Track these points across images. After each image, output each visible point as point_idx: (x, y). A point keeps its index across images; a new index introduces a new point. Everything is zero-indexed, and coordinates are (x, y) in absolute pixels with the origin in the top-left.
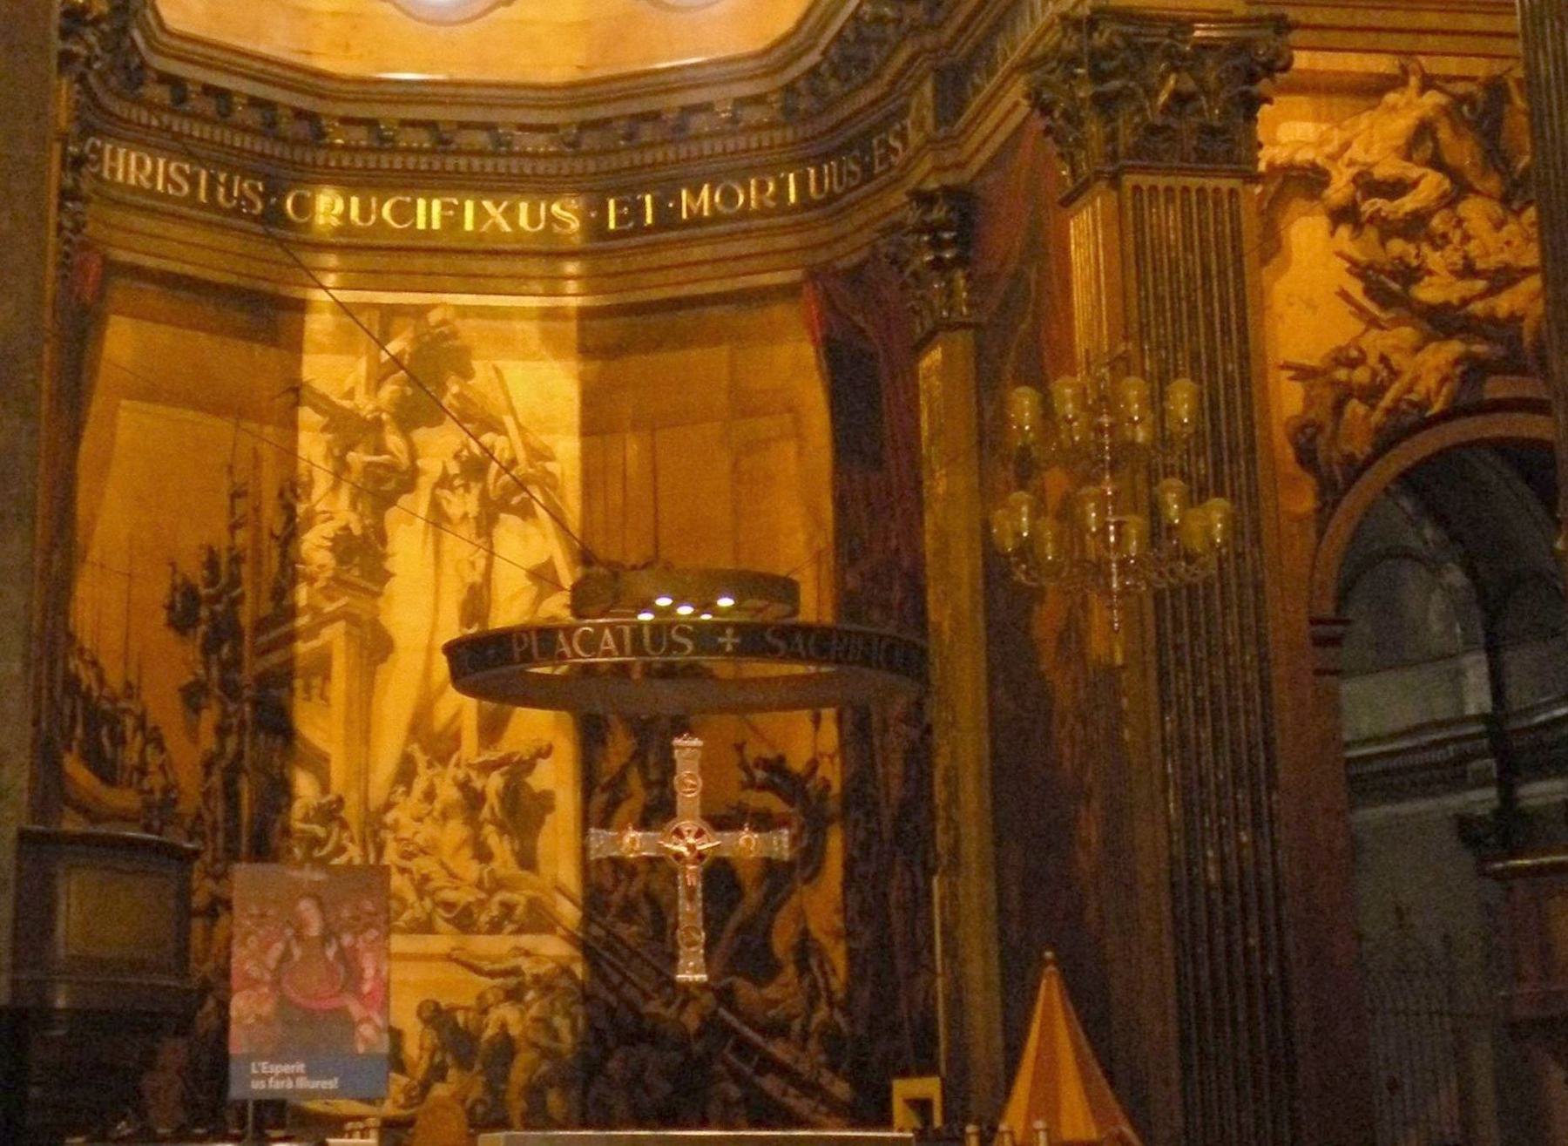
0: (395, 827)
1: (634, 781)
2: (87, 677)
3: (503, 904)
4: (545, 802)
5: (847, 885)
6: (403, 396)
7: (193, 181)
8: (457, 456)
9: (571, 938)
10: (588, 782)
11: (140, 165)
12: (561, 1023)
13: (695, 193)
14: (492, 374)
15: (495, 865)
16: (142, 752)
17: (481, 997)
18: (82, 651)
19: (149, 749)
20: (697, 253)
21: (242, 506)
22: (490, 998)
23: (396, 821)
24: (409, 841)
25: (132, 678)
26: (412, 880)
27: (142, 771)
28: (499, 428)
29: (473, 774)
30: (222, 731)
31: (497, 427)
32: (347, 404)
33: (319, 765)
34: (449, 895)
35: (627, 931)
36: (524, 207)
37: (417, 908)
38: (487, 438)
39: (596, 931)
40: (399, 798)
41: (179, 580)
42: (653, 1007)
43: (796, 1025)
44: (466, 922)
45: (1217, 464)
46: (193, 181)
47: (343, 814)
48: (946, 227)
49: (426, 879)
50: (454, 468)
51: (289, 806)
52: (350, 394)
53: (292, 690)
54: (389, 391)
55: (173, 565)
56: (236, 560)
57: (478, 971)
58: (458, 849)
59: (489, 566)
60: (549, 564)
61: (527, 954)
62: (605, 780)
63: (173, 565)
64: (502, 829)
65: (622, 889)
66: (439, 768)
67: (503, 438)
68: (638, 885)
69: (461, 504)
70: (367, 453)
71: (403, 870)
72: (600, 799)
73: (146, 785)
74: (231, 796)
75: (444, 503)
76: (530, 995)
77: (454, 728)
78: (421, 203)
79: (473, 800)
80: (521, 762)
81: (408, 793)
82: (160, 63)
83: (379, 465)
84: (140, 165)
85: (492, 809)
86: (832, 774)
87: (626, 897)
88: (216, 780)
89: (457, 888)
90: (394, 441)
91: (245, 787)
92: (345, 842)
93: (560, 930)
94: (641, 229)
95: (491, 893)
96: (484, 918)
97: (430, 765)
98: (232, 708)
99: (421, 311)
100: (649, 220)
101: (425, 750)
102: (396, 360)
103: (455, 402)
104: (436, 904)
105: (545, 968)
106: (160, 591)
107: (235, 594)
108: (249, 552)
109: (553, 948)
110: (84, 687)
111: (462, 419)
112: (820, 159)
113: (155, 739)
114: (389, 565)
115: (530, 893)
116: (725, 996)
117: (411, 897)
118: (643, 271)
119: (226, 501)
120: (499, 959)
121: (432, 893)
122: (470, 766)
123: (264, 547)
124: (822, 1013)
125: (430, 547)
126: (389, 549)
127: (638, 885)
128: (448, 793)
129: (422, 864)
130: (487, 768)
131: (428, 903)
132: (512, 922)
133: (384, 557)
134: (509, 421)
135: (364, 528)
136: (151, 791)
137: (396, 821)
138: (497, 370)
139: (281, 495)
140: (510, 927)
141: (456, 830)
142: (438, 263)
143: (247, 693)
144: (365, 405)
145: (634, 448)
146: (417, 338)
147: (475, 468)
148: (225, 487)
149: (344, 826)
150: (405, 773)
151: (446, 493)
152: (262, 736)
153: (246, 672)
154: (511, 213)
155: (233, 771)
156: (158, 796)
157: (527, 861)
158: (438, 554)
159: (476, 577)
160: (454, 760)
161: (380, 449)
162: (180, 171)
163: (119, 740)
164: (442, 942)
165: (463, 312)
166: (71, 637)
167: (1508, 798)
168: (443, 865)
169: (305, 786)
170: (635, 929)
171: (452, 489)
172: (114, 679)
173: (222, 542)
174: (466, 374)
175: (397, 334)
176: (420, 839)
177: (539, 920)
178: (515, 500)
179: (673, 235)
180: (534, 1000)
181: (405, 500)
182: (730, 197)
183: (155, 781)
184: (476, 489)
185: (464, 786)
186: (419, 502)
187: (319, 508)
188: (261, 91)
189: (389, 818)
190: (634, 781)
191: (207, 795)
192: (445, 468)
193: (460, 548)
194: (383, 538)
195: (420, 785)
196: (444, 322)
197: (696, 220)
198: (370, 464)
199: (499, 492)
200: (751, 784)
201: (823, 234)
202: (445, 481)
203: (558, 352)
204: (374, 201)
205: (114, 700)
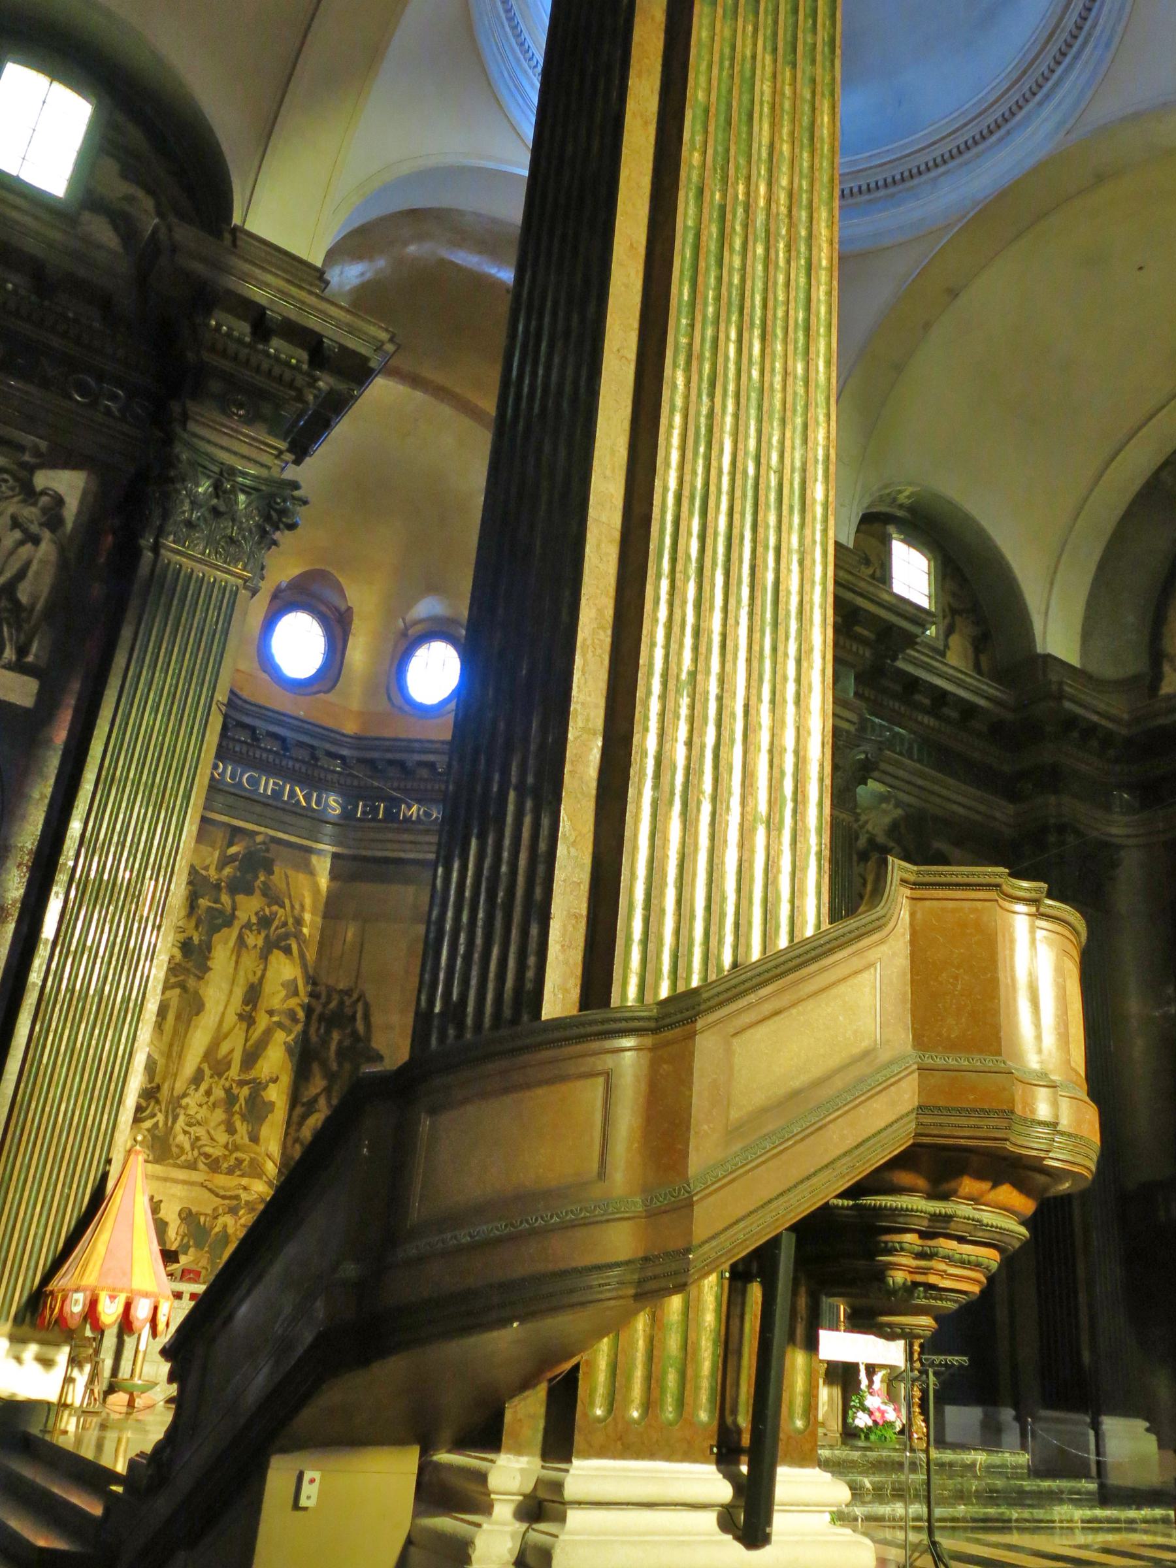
0: (186, 1108)
1: (322, 1102)
3: (236, 1159)
6: (235, 877)
8: (257, 914)
9: (269, 1183)
10: (294, 1100)
14: (283, 876)
15: (237, 1137)
17: (215, 1210)
20: (406, 837)
23: (188, 1104)
26: (190, 1138)
29: (234, 1085)
32: (204, 872)
34: (208, 1150)
37: (190, 1156)
38: (275, 908)
47: (158, 1095)
49: (198, 1139)
50: (254, 920)
52: (206, 868)
54: (228, 871)
57: (217, 1195)
58: (219, 1124)
59: (263, 976)
61: (245, 1188)
62: (305, 1100)
64: (244, 1118)
67: (282, 910)
69: (255, 940)
70: (209, 901)
71: (185, 1132)
72: (299, 1110)
75: (246, 937)
76: (241, 1212)
77: (226, 1060)
79: (231, 1099)
81: (196, 1090)
83: (216, 909)
85: (241, 1105)
90: (225, 898)
92: (156, 1111)
93: (264, 1178)
94: (375, 819)
95: (231, 1152)
96: (225, 1165)
97: (212, 1077)
99: (254, 834)
100: (381, 816)
101: (210, 1068)
102: (233, 858)
103: (261, 886)
104: (200, 1154)
111: (265, 894)
114: (209, 963)
115: (253, 1155)
117: (187, 1147)
118: (373, 840)
120: (229, 1189)
122: (233, 1080)
125: (234, 958)
126: (211, 955)
128: (219, 1093)
129: (199, 1131)
130: (242, 1083)
131: (196, 1153)
132: (240, 1170)
133: (208, 958)
134: (287, 901)
135: (200, 940)
137: (188, 1104)
138: (287, 876)
141: (219, 1115)
144: (212, 874)
146: (247, 848)
147: (265, 922)
149: (158, 1102)
150: (197, 1079)
151: (248, 932)
157: (254, 1139)
158: (237, 962)
159: (256, 980)
160: (225, 1077)
161: (217, 901)
164: (196, 1176)
165: (274, 840)
168: (208, 1132)
171: (251, 931)
174: (270, 872)
175: (237, 844)
176: (199, 1117)
177: (256, 1170)
178: (283, 944)
180: (244, 1215)
181: (225, 930)
184: (263, 934)
185: (228, 1091)
186: (234, 933)
189: (184, 1102)
192: (249, 920)
193: (249, 961)
194: (209, 949)
195: (203, 1087)
196: (264, 843)
197: (407, 820)
199: (275, 938)
202: (248, 926)
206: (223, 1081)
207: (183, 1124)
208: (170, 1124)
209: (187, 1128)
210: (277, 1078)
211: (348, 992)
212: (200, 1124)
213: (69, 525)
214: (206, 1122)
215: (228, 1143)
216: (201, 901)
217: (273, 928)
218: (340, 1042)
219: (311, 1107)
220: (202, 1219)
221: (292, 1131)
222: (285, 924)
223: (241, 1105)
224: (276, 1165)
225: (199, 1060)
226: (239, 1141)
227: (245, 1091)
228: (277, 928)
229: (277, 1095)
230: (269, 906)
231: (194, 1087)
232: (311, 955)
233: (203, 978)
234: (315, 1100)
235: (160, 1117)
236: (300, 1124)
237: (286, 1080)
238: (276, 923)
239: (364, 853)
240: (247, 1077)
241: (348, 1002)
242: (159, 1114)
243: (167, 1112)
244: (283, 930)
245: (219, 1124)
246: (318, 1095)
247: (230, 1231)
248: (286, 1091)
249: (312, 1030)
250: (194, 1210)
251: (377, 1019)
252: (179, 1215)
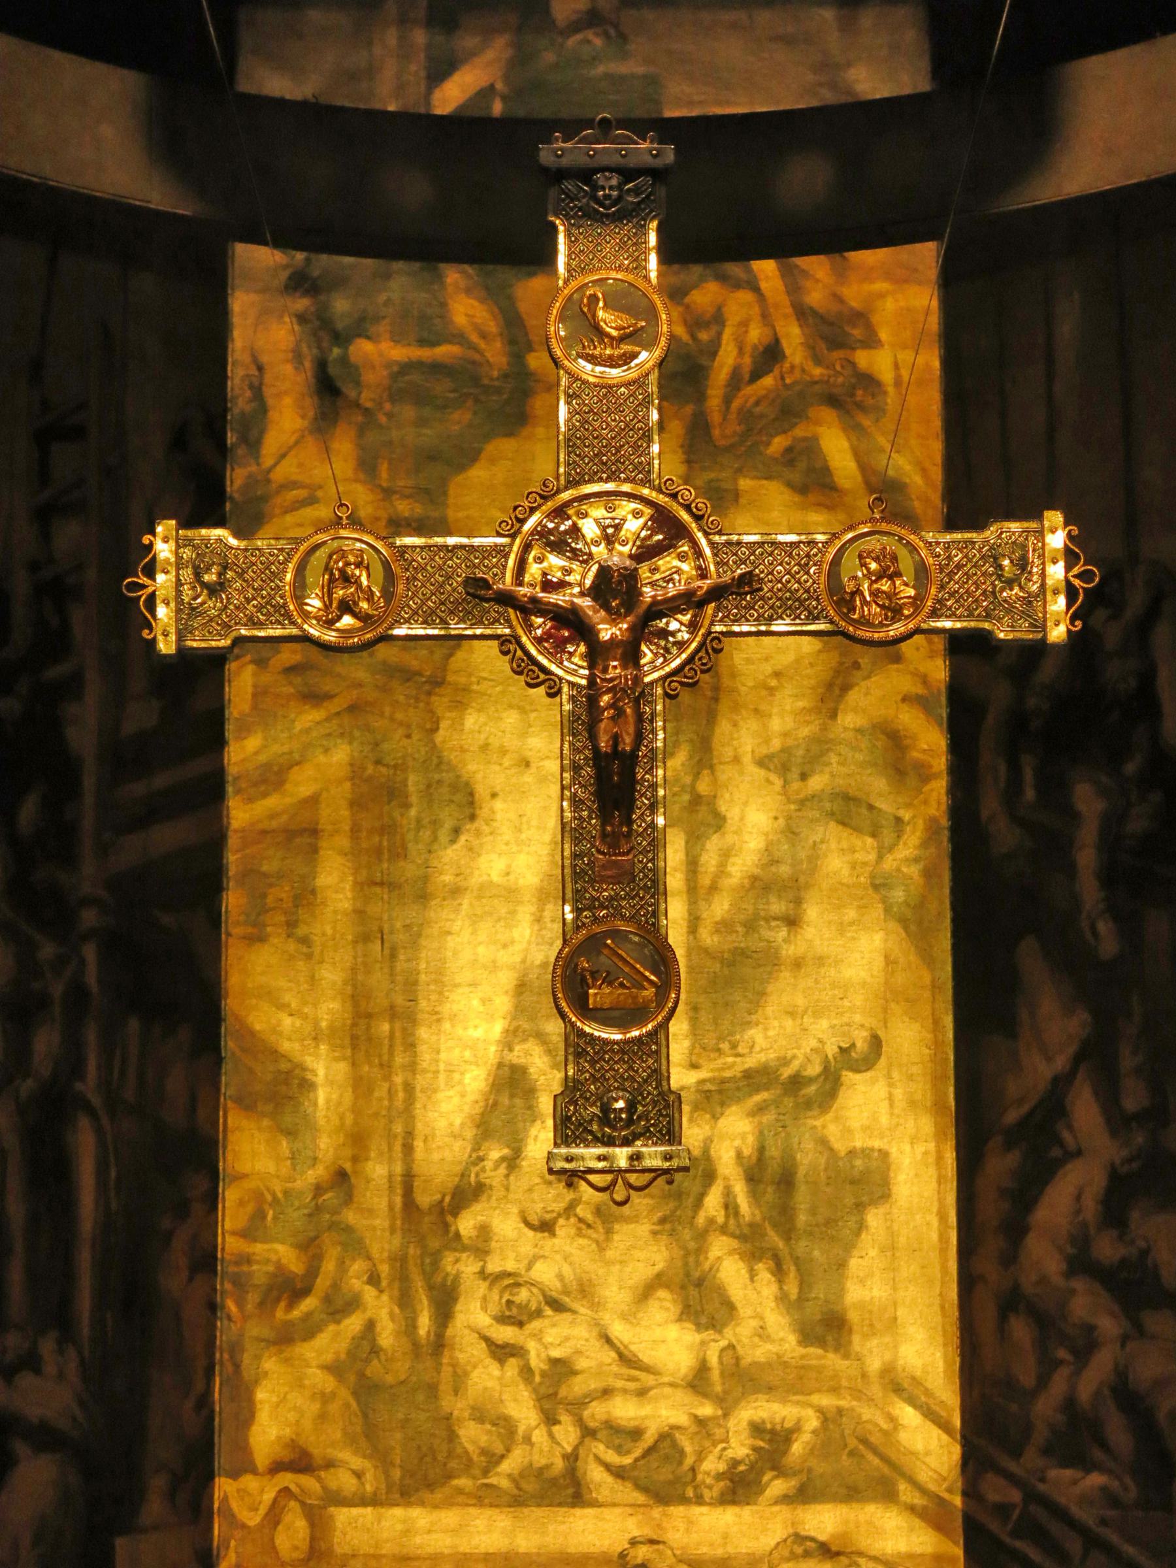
0: (481, 1246)
15: (741, 1332)
24: (508, 1281)
26: (526, 1372)
34: (624, 1410)
39: (996, 1490)
40: (494, 1176)
44: (665, 1474)
47: (350, 1217)
49: (561, 1369)
51: (212, 1199)
53: (215, 920)
58: (646, 1292)
62: (1012, 1116)
65: (1058, 1385)
67: (745, 296)
68: (1102, 1365)
70: (397, 338)
71: (501, 1352)
80: (796, 1082)
81: (512, 1162)
83: (436, 368)
85: (728, 1193)
87: (1070, 1404)
89: (642, 1393)
92: (356, 1282)
95: (727, 1405)
96: (712, 1465)
98: (47, 951)
104: (588, 1433)
107: (55, 672)
115: (826, 1401)
121: (577, 1406)
127: (1102, 1365)
131: (567, 1434)
132: (781, 1471)
137: (484, 1231)
139: (179, 441)
140: (777, 1487)
143: (89, 918)
149: (353, 1244)
152: (134, 1025)
153: (88, 867)
170: (1096, 1479)
176: (545, 1273)
187: (278, 475)
189: (466, 1224)
198: (407, 367)
207: (483, 1320)
208: (425, 1323)
209: (506, 1334)
210: (876, 1043)
212: (557, 1306)
214: (585, 1290)
215: (703, 1368)
216: (362, 349)
218: (1111, 825)
221: (988, 1267)
222: (771, 354)
223: (728, 1193)
224: (945, 1426)
225: (497, 1029)
226: (758, 1353)
228: (735, 382)
231: (495, 1153)
233: (437, 682)
238: (727, 358)
240: (734, 1065)
242: (369, 1293)
243: (402, 1278)
244: (768, 381)
245: (646, 1292)
246: (1061, 1084)
248: (922, 1089)
249: (990, 805)
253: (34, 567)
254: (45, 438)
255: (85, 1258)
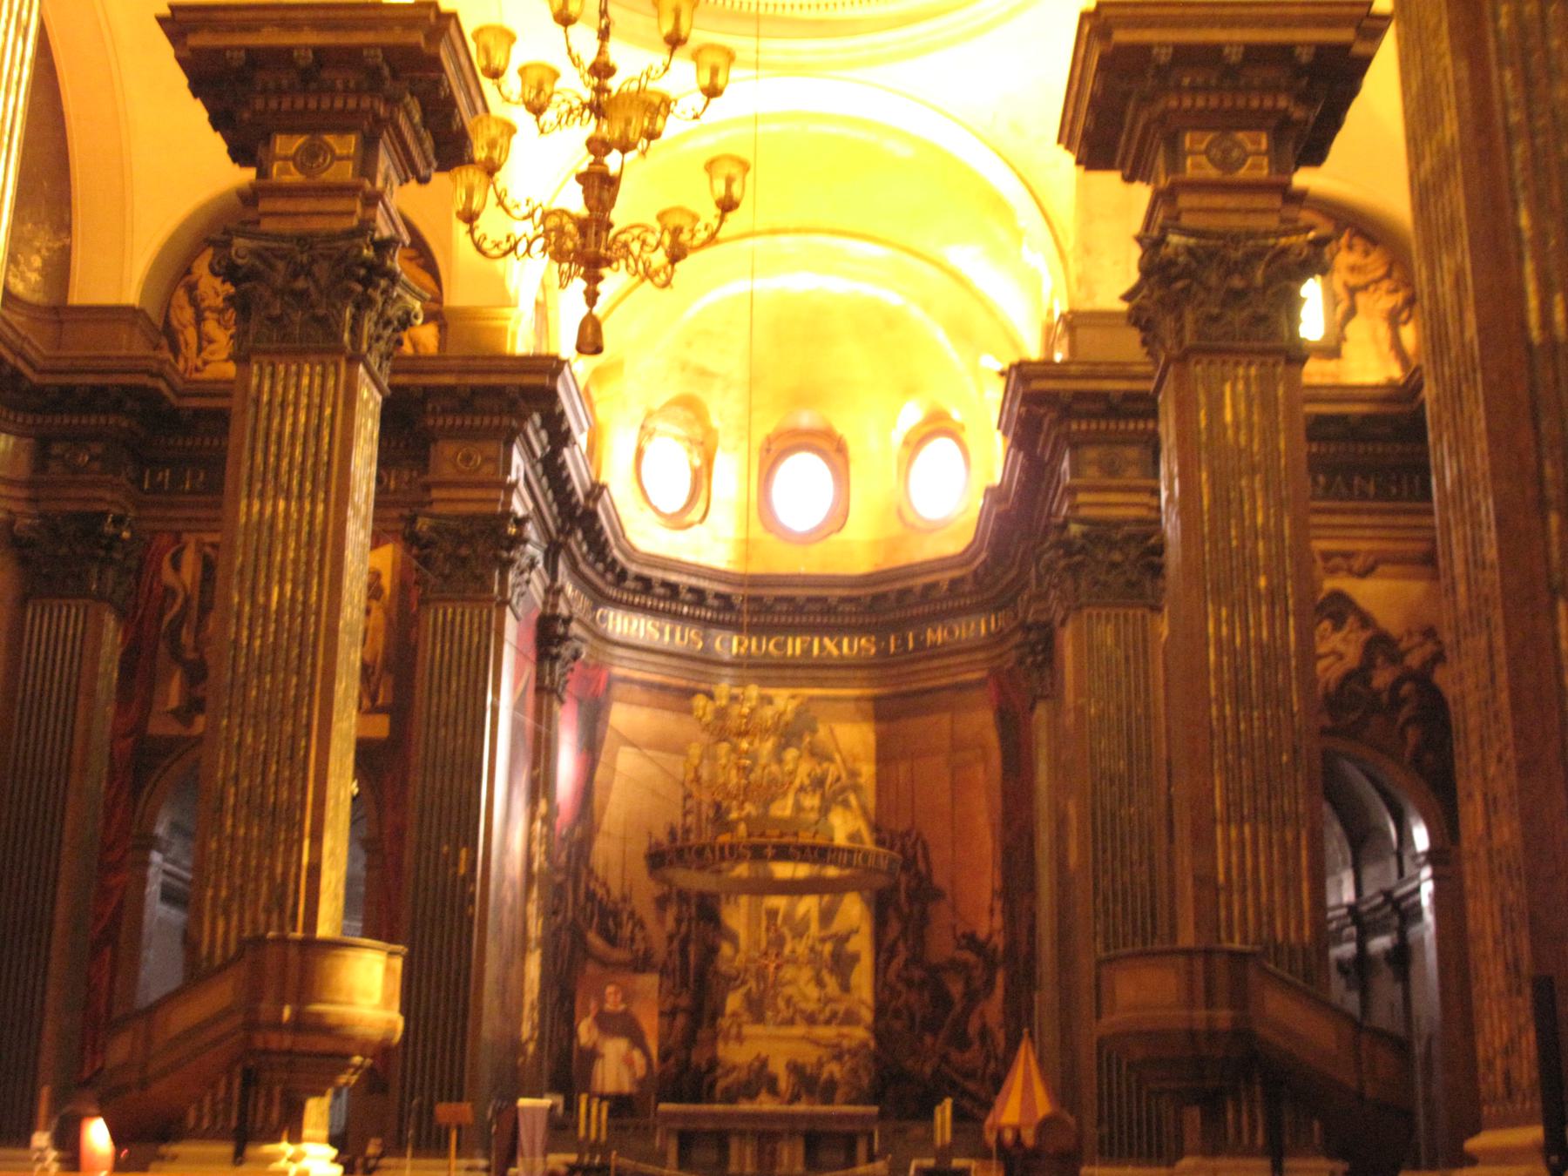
2: (600, 892)
4: (855, 958)
5: (1005, 1000)
7: (662, 632)
9: (867, 1028)
11: (630, 623)
12: (861, 1072)
13: (935, 631)
16: (632, 932)
17: (820, 1058)
18: (597, 879)
19: (637, 930)
21: (690, 803)
22: (825, 1059)
25: (627, 891)
27: (632, 940)
28: (831, 759)
30: (679, 921)
31: (831, 759)
33: (733, 938)
35: (897, 1025)
36: (845, 642)
37: (786, 1013)
38: (825, 765)
41: (653, 840)
42: (910, 1063)
43: (980, 1072)
45: (1130, 764)
46: (662, 632)
48: (1037, 643)
50: (807, 782)
55: (650, 834)
56: (687, 831)
60: (859, 831)
63: (650, 834)
64: (831, 971)
65: (894, 1003)
66: (797, 941)
72: (883, 956)
73: (635, 947)
74: (683, 951)
78: (790, 641)
82: (633, 568)
84: (630, 623)
86: (999, 941)
88: (676, 944)
91: (692, 949)
92: (748, 977)
94: (906, 651)
97: (794, 938)
101: (791, 929)
105: (854, 1044)
106: (643, 847)
108: (694, 827)
109: (860, 1034)
110: (599, 896)
112: (997, 610)
113: (640, 924)
116: (945, 1058)
119: (680, 802)
123: (703, 825)
124: (992, 1065)
130: (823, 940)
131: (791, 1010)
134: (837, 757)
136: (638, 950)
138: (832, 731)
142: (800, 673)
145: (903, 768)
147: (818, 783)
148: (680, 793)
154: (839, 646)
155: (685, 942)
156: (641, 953)
157: (845, 987)
162: (654, 626)
163: (619, 925)
164: (799, 1030)
165: (811, 699)
166: (591, 872)
167: (1362, 946)
169: (726, 949)
172: (616, 892)
173: (679, 821)
174: (814, 731)
177: (850, 1018)
178: (840, 798)
179: (924, 653)
182: (951, 632)
183: (640, 946)
185: (812, 949)
188: (693, 581)
190: (901, 946)
191: (670, 954)
200: (959, 947)
201: (997, 651)
202: (802, 789)
203: (865, 719)
204: (764, 642)
205: (615, 904)
206: (804, 940)
211: (908, 834)
213: (387, 592)
217: (827, 786)
219: (892, 953)
220: (809, 1070)
222: (838, 779)
227: (828, 948)
228: (831, 785)
229: (862, 944)
230: (820, 764)
232: (871, 802)
234: (895, 943)
235: (752, 984)
236: (886, 968)
237: (866, 929)
239: (904, 688)
241: (909, 844)
247: (838, 1075)
250: (800, 1060)
251: (935, 856)
252: (787, 1066)
253: (683, 825)
254: (687, 797)
255: (692, 972)
